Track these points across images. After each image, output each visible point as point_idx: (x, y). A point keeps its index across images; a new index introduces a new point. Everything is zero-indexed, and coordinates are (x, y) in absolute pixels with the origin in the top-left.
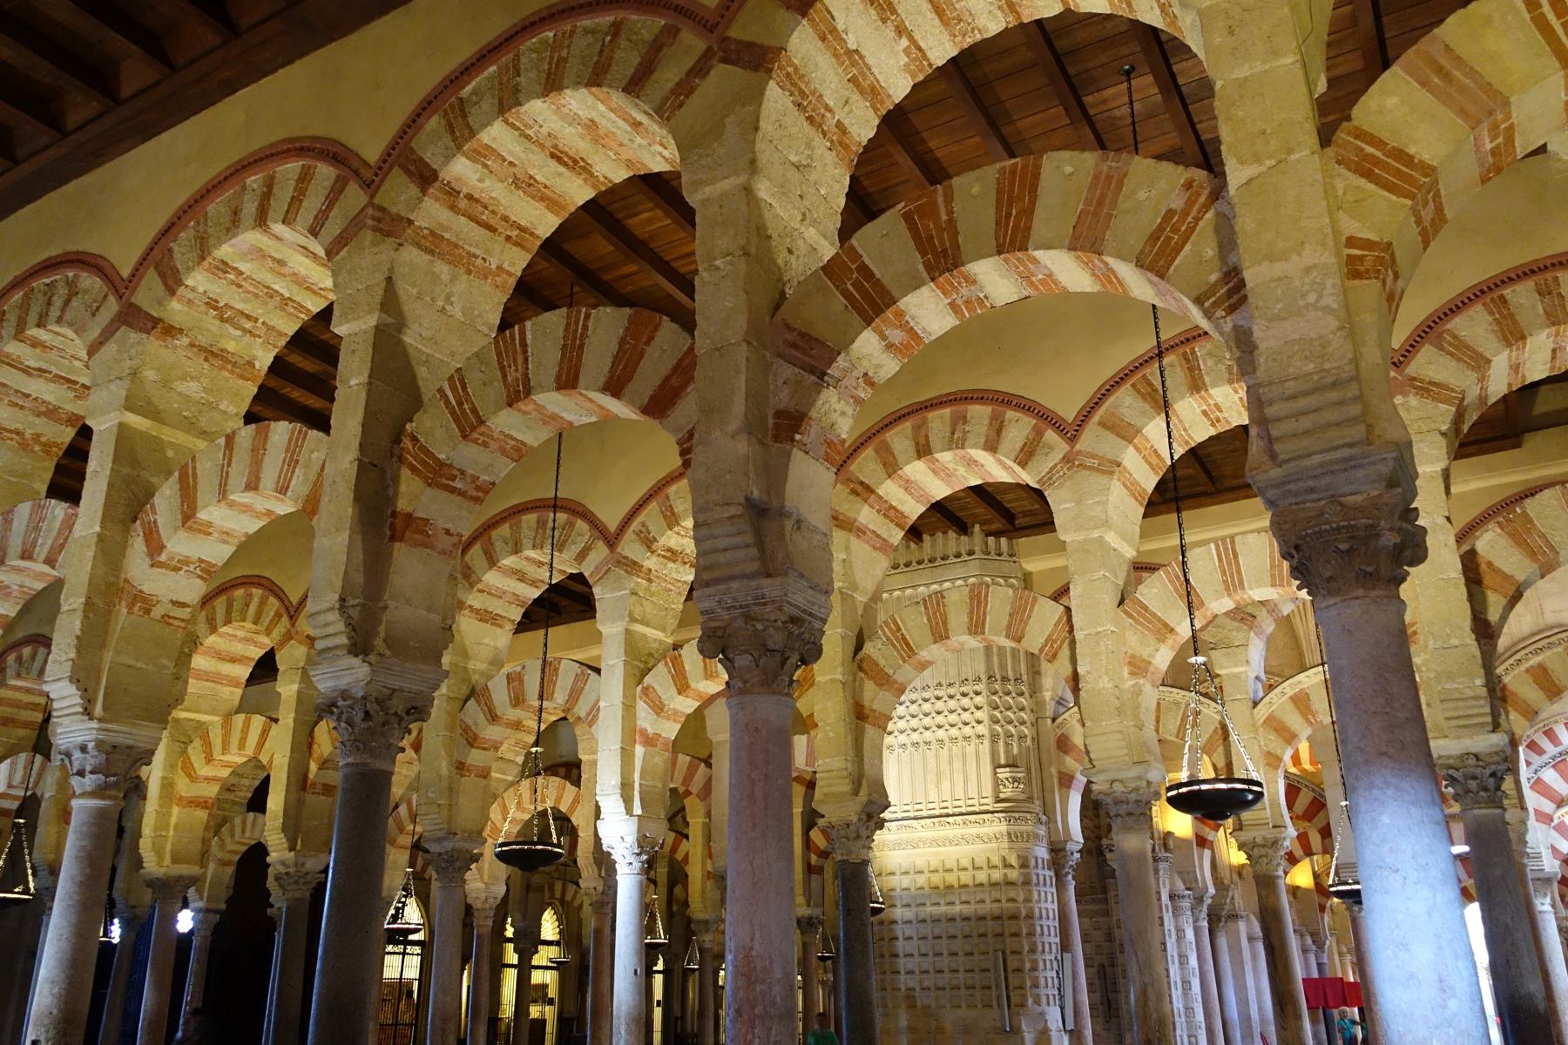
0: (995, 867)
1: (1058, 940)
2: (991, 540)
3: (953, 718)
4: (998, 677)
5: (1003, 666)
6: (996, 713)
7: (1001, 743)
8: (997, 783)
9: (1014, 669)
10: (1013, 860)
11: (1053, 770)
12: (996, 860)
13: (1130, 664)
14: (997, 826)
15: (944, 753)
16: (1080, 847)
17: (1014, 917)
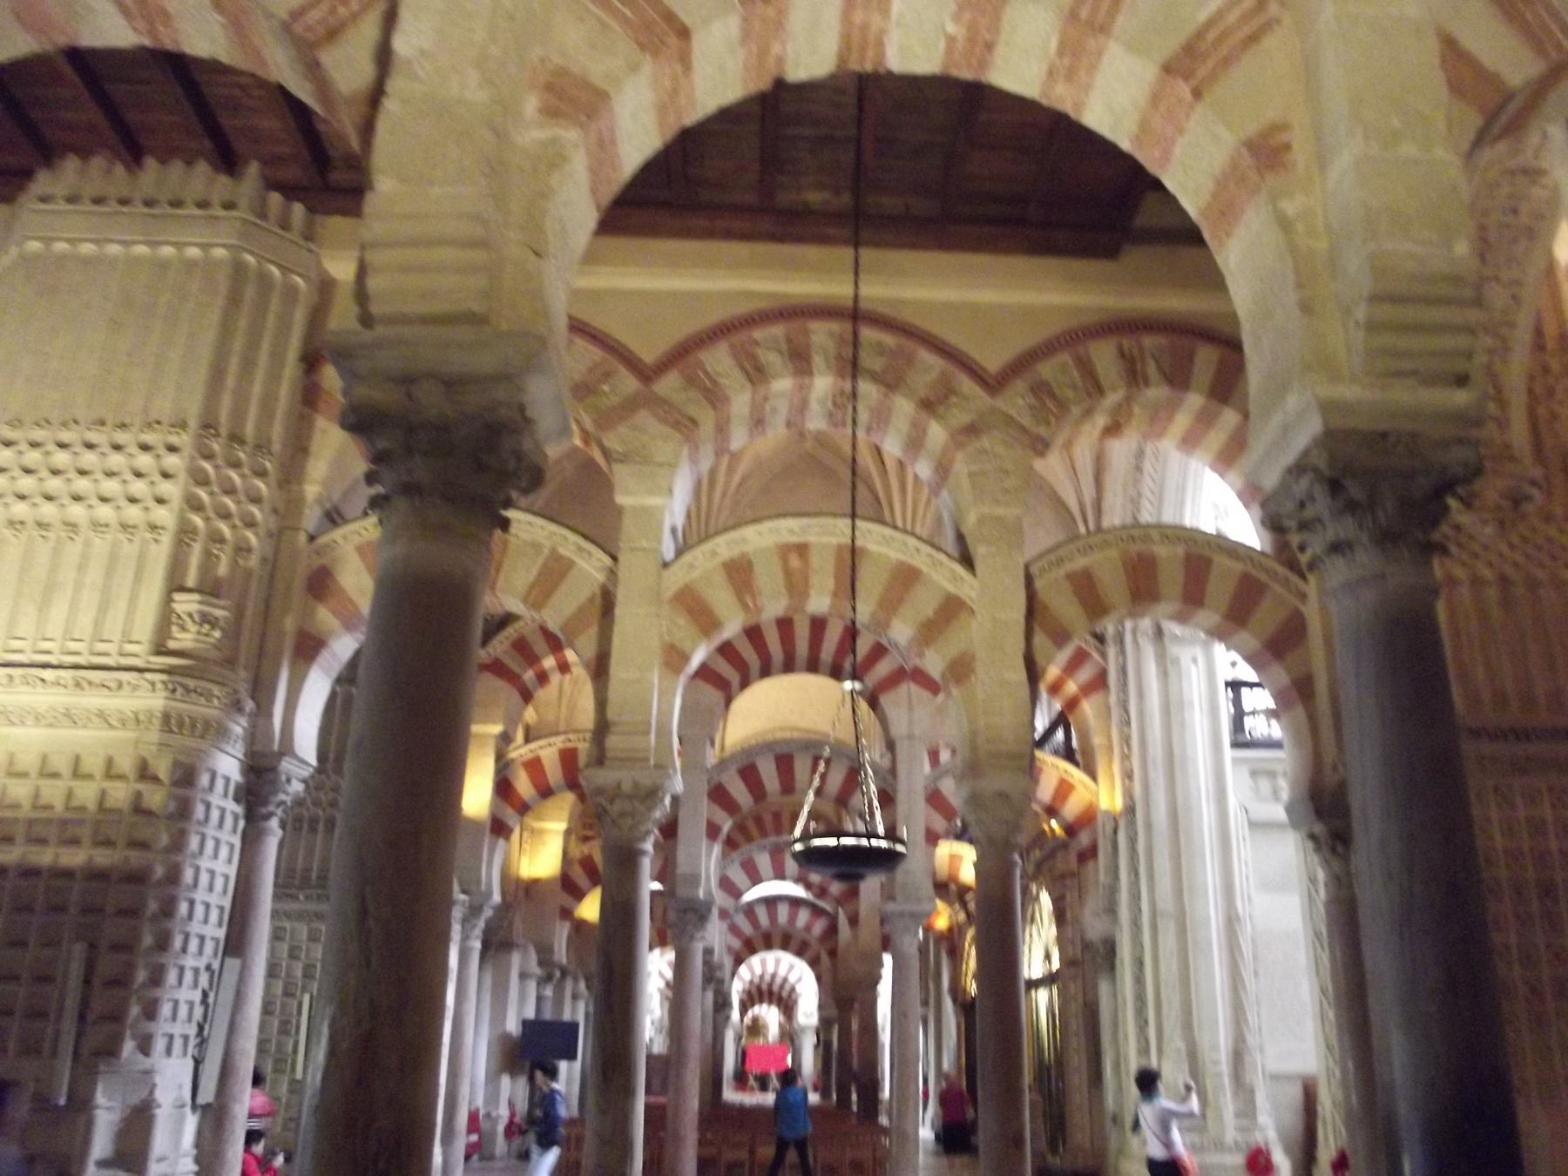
0: (121, 777)
1: (221, 933)
2: (275, 198)
3: (110, 486)
4: (224, 431)
5: (238, 414)
6: (202, 494)
7: (197, 549)
8: (166, 620)
9: (258, 429)
10: (162, 768)
11: (289, 624)
12: (126, 764)
13: (549, 88)
14: (150, 699)
15: (73, 551)
16: (306, 773)
17: (138, 878)
